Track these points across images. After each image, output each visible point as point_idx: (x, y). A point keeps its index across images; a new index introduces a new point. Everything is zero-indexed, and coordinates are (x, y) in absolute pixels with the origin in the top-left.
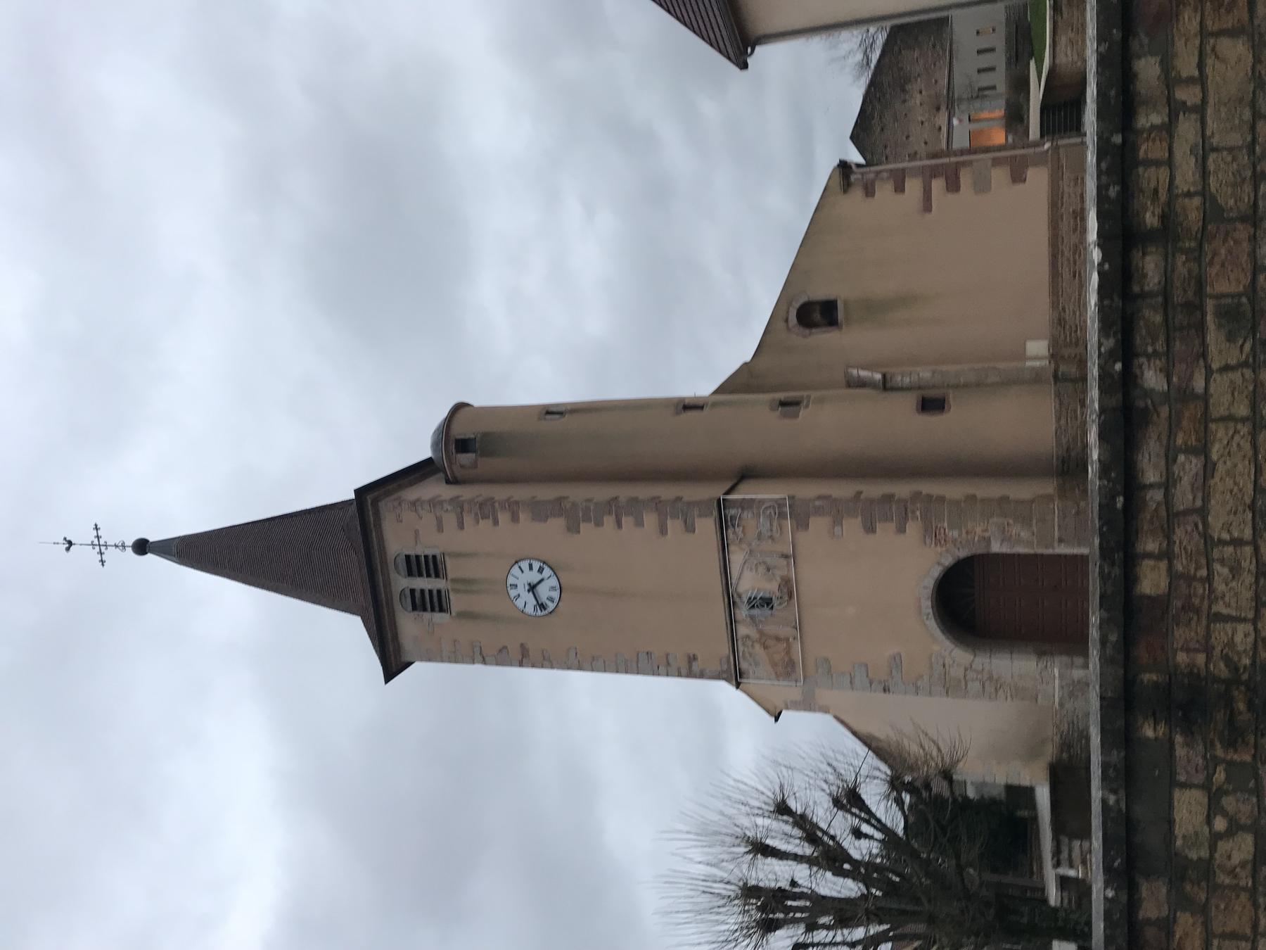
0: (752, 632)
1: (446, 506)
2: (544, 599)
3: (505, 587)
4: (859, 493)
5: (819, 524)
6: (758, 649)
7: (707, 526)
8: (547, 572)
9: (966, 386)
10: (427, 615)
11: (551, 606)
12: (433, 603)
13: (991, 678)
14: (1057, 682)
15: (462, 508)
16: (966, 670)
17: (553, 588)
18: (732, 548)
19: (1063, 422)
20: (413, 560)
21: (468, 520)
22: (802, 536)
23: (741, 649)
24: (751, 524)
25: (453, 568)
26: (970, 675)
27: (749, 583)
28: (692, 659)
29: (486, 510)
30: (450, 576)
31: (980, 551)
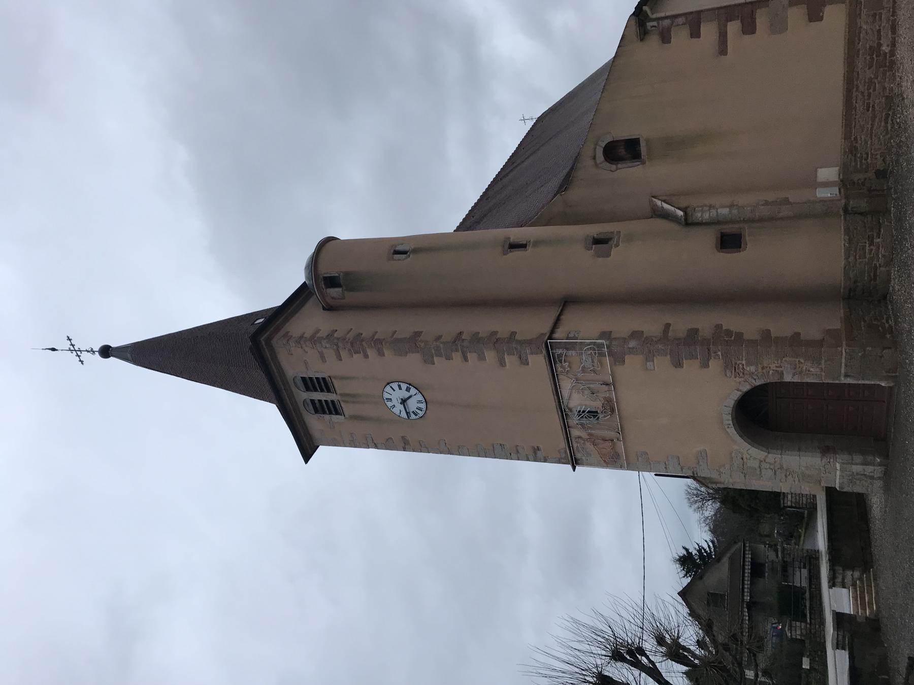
0: (584, 434)
1: (324, 343)
3: (383, 401)
4: (668, 326)
5: (633, 362)
6: (589, 446)
7: (538, 361)
8: (413, 391)
9: (761, 220)
10: (327, 417)
11: (421, 413)
13: (781, 468)
14: (838, 473)
15: (337, 345)
16: (761, 461)
17: (419, 402)
18: (561, 377)
19: (851, 259)
21: (344, 354)
22: (620, 370)
23: (575, 445)
24: (578, 360)
26: (764, 465)
27: (577, 401)
28: (536, 450)
29: (357, 344)
30: (338, 392)
31: (774, 379)
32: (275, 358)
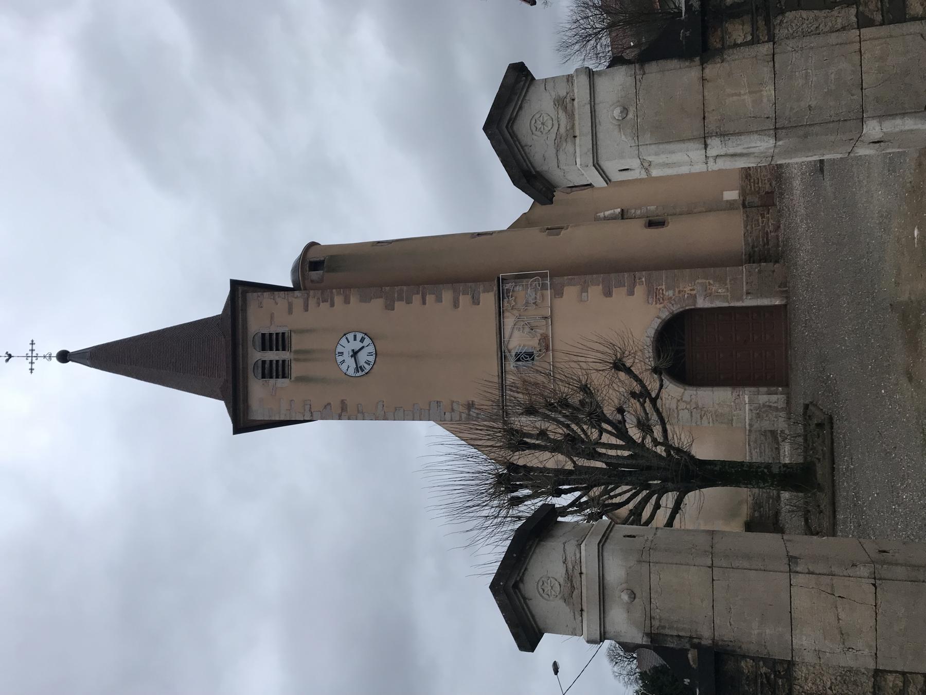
2: (362, 363)
5: (571, 292)
7: (488, 299)
8: (367, 341)
10: (272, 381)
11: (368, 368)
12: (276, 371)
17: (370, 354)
18: (507, 314)
20: (267, 337)
22: (558, 302)
25: (297, 342)
30: (293, 349)
32: (244, 310)
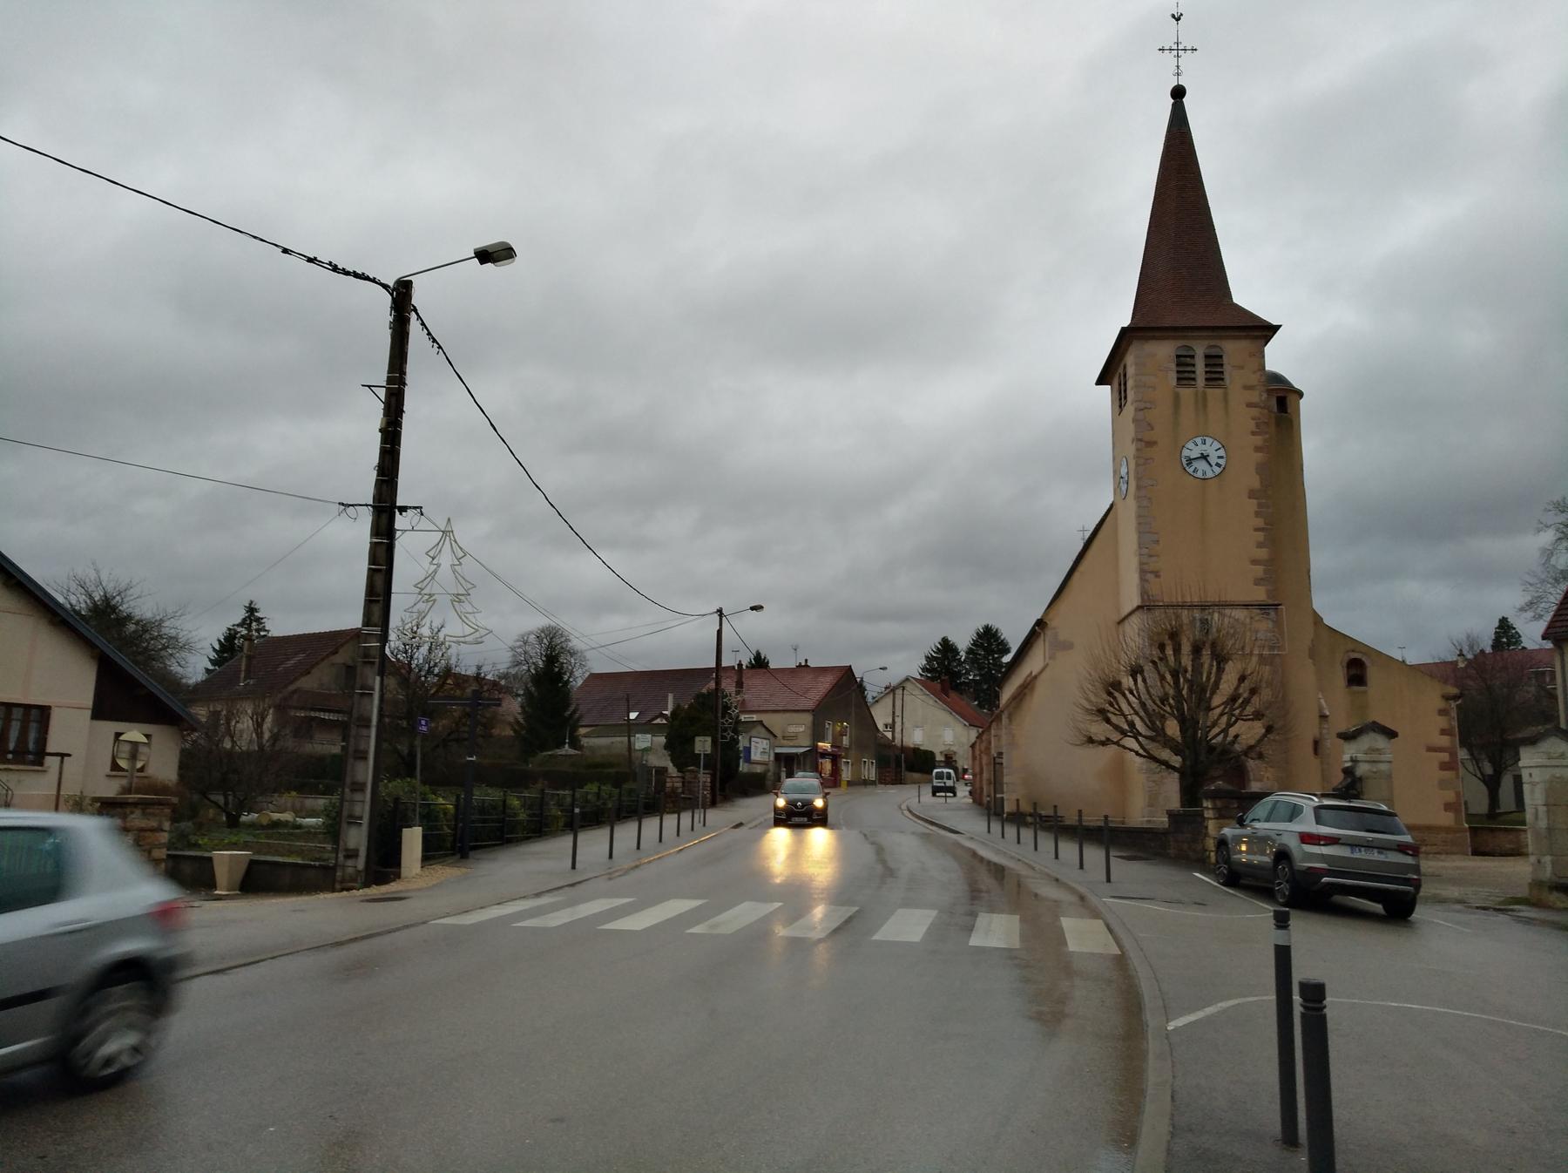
2: (1195, 464)
7: (1260, 594)
10: (1173, 366)
11: (1190, 470)
17: (1204, 473)
20: (1217, 361)
25: (1214, 394)
30: (1209, 391)
32: (1246, 338)
